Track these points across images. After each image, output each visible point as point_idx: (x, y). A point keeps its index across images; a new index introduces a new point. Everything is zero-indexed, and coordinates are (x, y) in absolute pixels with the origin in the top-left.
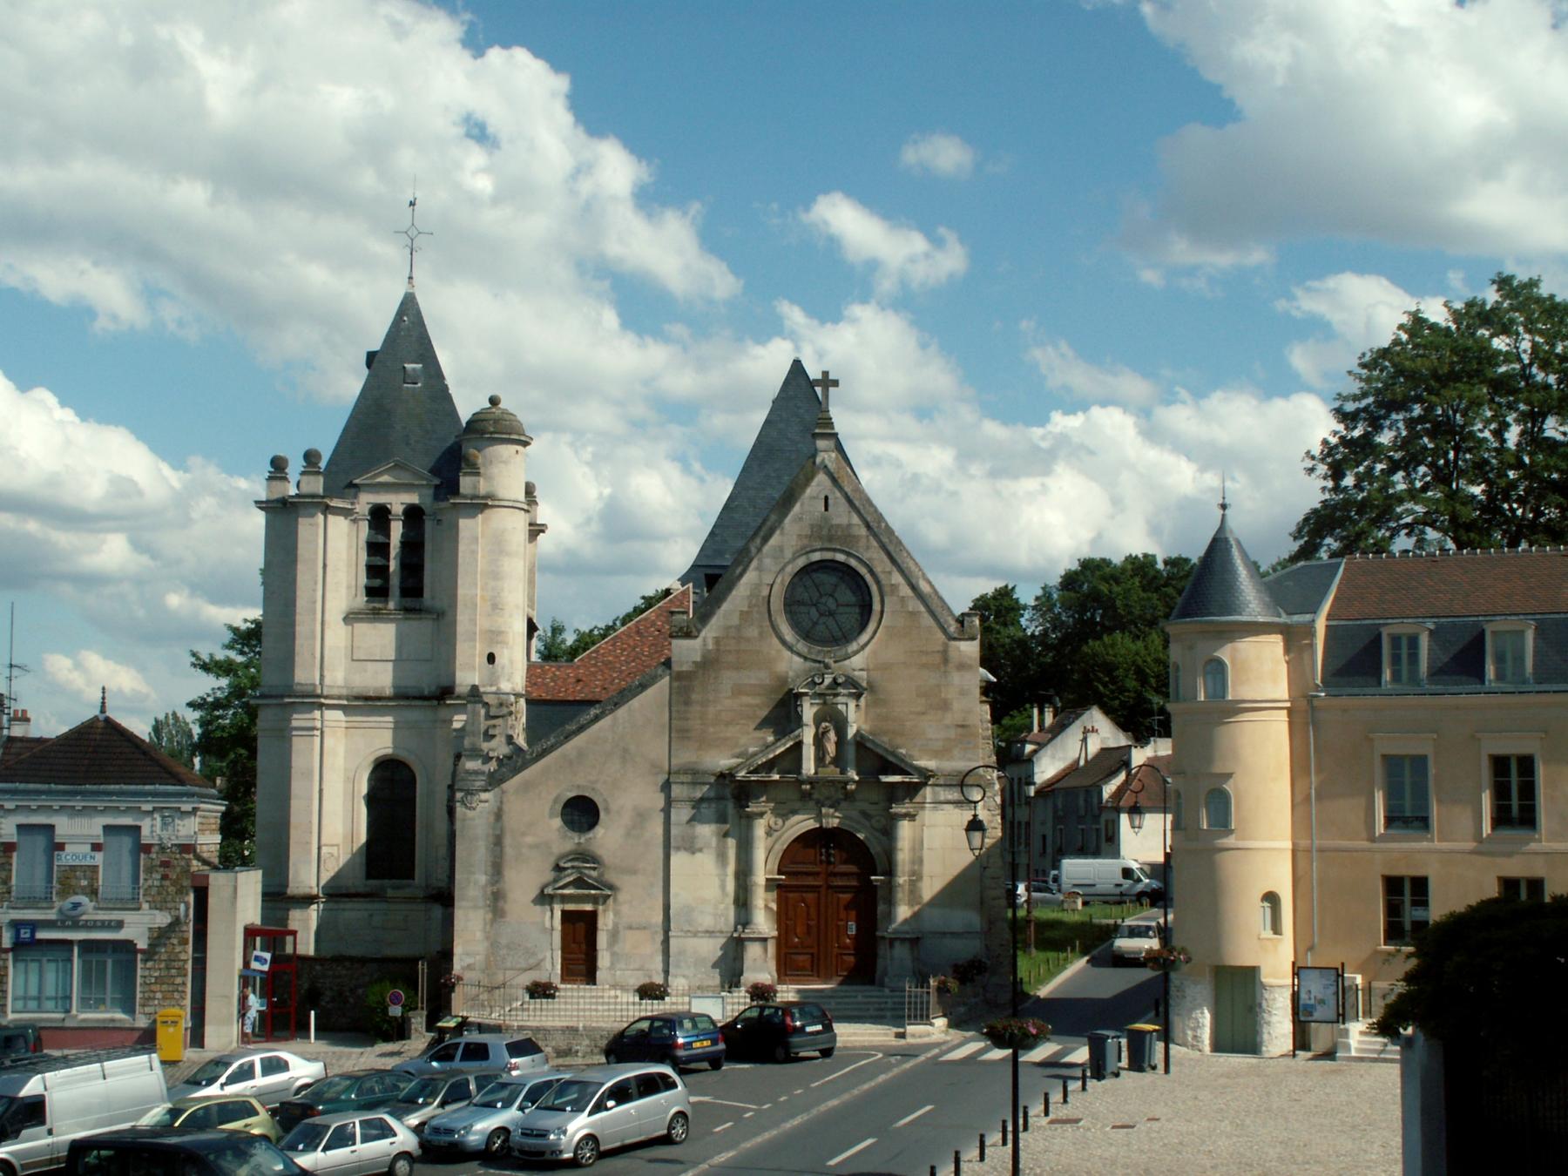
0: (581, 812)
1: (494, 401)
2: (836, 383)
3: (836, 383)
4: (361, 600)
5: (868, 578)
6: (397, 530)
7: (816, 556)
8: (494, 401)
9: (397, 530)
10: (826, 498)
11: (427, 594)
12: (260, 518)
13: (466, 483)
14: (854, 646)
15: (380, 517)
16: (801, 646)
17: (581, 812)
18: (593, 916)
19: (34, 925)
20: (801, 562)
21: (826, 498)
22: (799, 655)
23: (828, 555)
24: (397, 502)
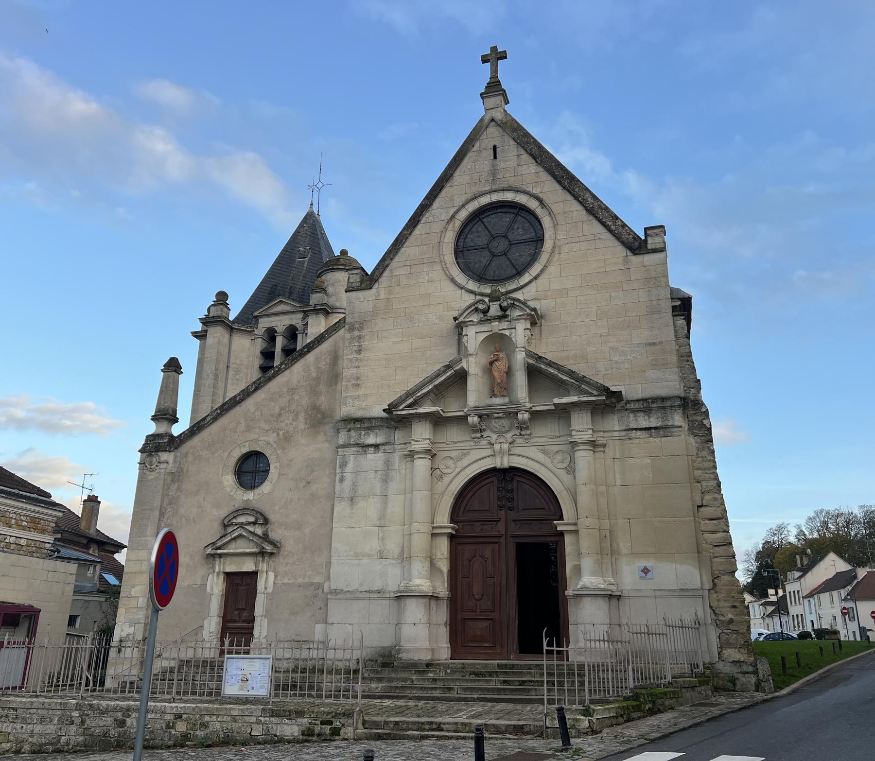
0: (251, 468)
2: (503, 56)
3: (503, 56)
5: (539, 211)
6: (280, 342)
7: (485, 200)
10: (495, 148)
14: (526, 278)
15: (271, 335)
16: (472, 285)
17: (251, 468)
18: (253, 575)
21: (495, 148)
22: (472, 292)
23: (495, 197)
24: (280, 324)
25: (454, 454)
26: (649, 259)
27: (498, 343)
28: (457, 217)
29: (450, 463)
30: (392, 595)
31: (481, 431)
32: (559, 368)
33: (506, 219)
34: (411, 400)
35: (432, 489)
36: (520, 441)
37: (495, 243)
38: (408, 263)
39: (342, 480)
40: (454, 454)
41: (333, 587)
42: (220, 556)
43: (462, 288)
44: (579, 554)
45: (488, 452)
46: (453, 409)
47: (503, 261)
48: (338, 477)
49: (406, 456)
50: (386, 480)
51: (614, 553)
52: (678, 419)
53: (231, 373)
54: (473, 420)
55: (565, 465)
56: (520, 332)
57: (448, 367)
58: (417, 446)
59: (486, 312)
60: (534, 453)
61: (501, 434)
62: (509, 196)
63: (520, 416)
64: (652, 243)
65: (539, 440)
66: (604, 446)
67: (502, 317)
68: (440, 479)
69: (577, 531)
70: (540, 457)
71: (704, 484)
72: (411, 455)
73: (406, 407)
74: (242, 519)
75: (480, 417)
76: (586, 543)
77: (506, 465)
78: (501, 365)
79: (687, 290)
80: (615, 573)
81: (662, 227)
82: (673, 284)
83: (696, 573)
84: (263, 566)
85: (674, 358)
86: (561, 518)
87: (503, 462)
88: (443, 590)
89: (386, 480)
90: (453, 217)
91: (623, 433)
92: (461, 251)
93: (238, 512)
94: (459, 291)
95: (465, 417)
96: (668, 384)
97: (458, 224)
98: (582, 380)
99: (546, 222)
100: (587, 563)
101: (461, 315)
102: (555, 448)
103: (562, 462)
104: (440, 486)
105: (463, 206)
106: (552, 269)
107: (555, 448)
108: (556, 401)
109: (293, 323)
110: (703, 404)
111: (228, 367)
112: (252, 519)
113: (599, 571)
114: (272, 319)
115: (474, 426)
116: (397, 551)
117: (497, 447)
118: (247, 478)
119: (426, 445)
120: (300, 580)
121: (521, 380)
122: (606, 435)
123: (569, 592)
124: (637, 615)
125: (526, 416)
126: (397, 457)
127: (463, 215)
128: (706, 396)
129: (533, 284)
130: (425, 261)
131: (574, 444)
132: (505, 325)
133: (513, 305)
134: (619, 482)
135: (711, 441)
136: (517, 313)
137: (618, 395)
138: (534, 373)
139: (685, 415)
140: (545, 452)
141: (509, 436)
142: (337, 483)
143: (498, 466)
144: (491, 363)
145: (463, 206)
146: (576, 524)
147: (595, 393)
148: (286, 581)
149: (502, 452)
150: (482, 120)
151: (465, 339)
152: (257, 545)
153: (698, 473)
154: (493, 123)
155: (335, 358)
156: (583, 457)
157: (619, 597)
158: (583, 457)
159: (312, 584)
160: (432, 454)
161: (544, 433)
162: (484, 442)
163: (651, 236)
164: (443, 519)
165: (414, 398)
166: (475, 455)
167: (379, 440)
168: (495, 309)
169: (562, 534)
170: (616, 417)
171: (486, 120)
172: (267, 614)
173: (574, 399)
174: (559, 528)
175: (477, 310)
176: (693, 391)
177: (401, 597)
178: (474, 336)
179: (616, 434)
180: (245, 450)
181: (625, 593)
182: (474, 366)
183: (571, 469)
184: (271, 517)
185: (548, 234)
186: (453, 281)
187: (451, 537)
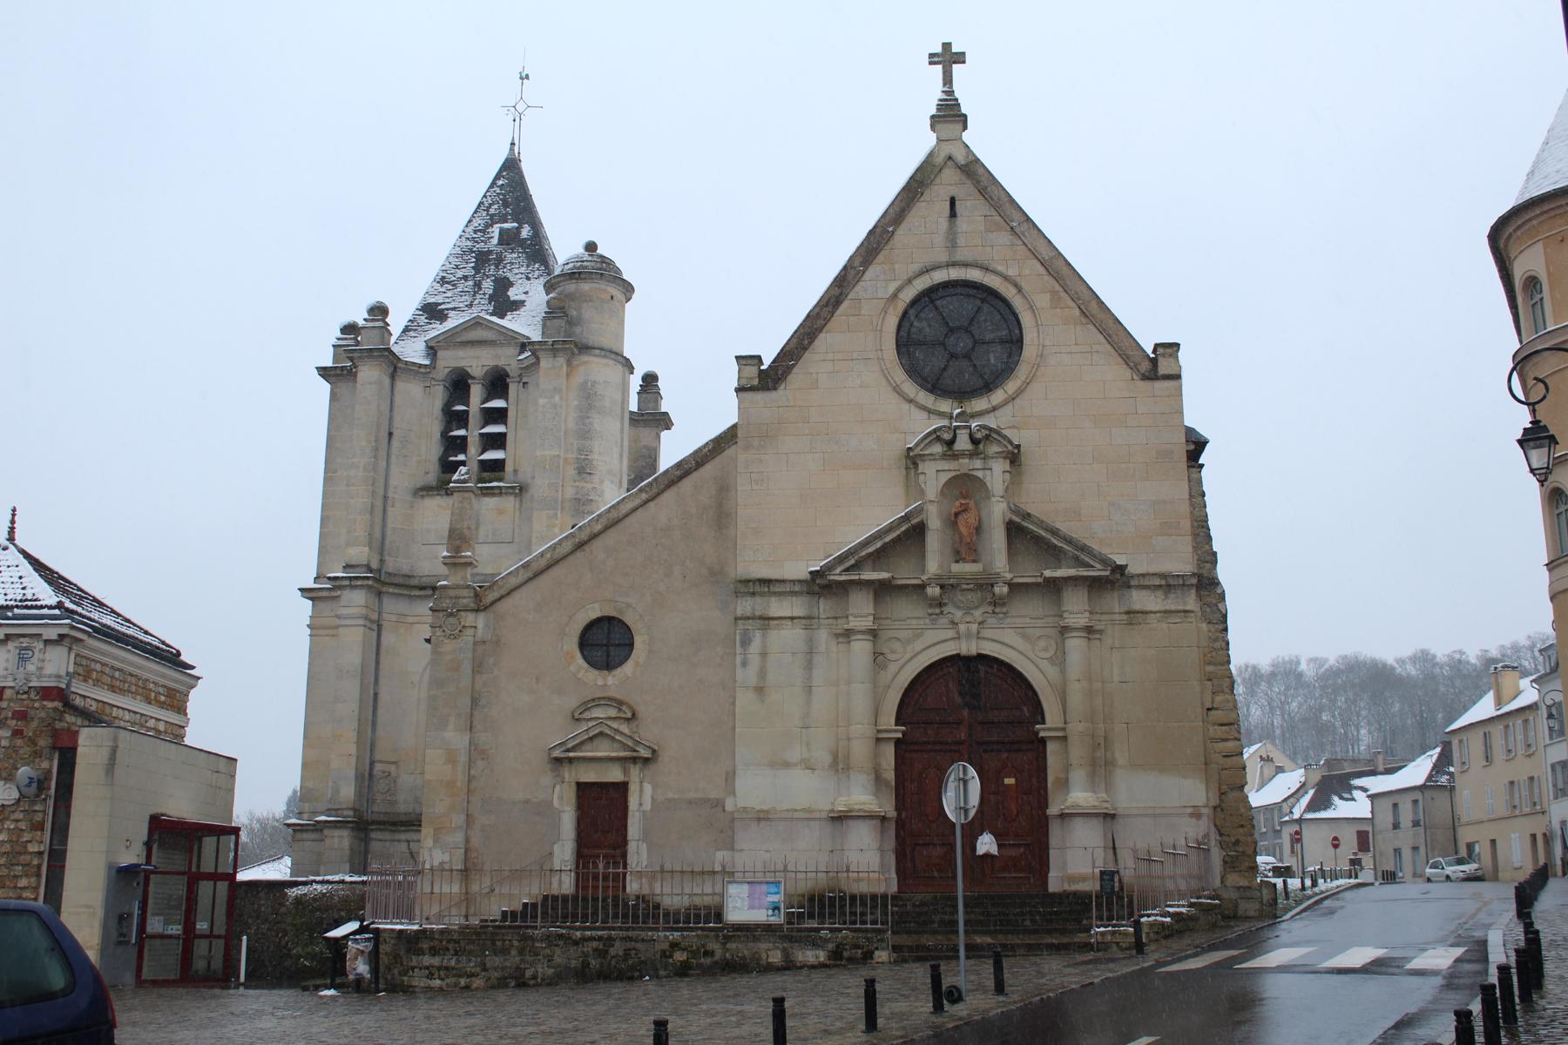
0: (606, 641)
1: (591, 247)
2: (960, 58)
3: (960, 58)
4: (432, 474)
7: (940, 276)
8: (591, 247)
10: (953, 201)
11: (509, 468)
12: (326, 387)
14: (998, 396)
17: (606, 641)
18: (622, 788)
20: (921, 284)
21: (953, 201)
23: (955, 274)
25: (903, 634)
26: (1160, 385)
27: (965, 488)
28: (901, 296)
29: (896, 645)
30: (824, 815)
31: (941, 605)
32: (1054, 532)
33: (969, 306)
34: (852, 562)
35: (874, 683)
36: (992, 621)
37: (952, 340)
38: (830, 356)
39: (744, 664)
40: (903, 634)
41: (741, 804)
42: (570, 760)
43: (910, 401)
44: (1067, 768)
45: (951, 634)
46: (905, 574)
47: (965, 363)
48: (739, 660)
49: (837, 636)
50: (809, 666)
51: (1109, 764)
52: (1191, 602)
53: (395, 443)
54: (933, 591)
55: (1048, 655)
56: (996, 475)
57: (906, 518)
58: (854, 623)
59: (950, 443)
60: (1010, 636)
61: (968, 610)
62: (974, 275)
63: (997, 590)
64: (1164, 367)
65: (1017, 620)
66: (1101, 632)
67: (973, 455)
68: (884, 667)
69: (1065, 738)
70: (1018, 642)
71: (1215, 682)
72: (848, 634)
73: (847, 570)
74: (598, 713)
75: (942, 587)
76: (1077, 751)
77: (974, 652)
78: (970, 518)
79: (1203, 431)
80: (1109, 786)
81: (1177, 345)
82: (1189, 422)
83: (1202, 787)
84: (635, 773)
85: (1186, 524)
86: (1043, 722)
87: (969, 648)
88: (888, 807)
89: (809, 666)
90: (895, 296)
91: (1125, 617)
92: (906, 344)
93: (596, 702)
94: (906, 406)
95: (922, 587)
97: (901, 306)
98: (1083, 548)
99: (1026, 320)
100: (1078, 776)
101: (917, 445)
102: (1038, 632)
103: (1046, 650)
104: (886, 676)
105: (910, 281)
106: (1036, 387)
107: (1038, 632)
108: (1048, 573)
109: (501, 363)
110: (1218, 583)
111: (390, 434)
112: (613, 713)
113: (1092, 787)
114: (461, 353)
115: (934, 599)
116: (828, 759)
117: (962, 627)
118: (599, 654)
119: (868, 623)
120: (692, 795)
121: (997, 539)
122: (1104, 617)
123: (1053, 810)
124: (1137, 837)
125: (1005, 589)
126: (823, 635)
127: (908, 295)
128: (1223, 573)
129: (1010, 406)
130: (855, 356)
131: (1064, 630)
132: (978, 463)
133: (987, 437)
134: (1116, 678)
135: (1226, 630)
136: (994, 449)
137: (1121, 569)
138: (1015, 531)
139: (1200, 597)
140: (1025, 637)
141: (978, 613)
142: (739, 670)
143: (964, 652)
144: (956, 515)
145: (910, 281)
146: (1064, 729)
147: (1098, 566)
148: (670, 795)
149: (969, 636)
150: (931, 155)
151: (921, 477)
152: (625, 747)
153: (1210, 668)
154: (950, 163)
155: (724, 489)
156: (1075, 644)
157: (1113, 816)
158: (1075, 644)
159: (706, 801)
160: (873, 634)
161: (1030, 611)
162: (943, 621)
163: (1163, 355)
164: (888, 719)
165: (856, 559)
166: (931, 636)
168: (963, 443)
169: (1043, 741)
170: (1116, 594)
171: (939, 160)
172: (646, 836)
173: (1072, 572)
174: (1042, 734)
175: (938, 439)
176: (1208, 566)
177: (840, 819)
178: (935, 476)
179: (1117, 617)
180: (594, 615)
181: (1120, 812)
182: (934, 523)
183: (1060, 659)
184: (642, 710)
185: (1029, 337)
186: (897, 390)
187: (898, 742)
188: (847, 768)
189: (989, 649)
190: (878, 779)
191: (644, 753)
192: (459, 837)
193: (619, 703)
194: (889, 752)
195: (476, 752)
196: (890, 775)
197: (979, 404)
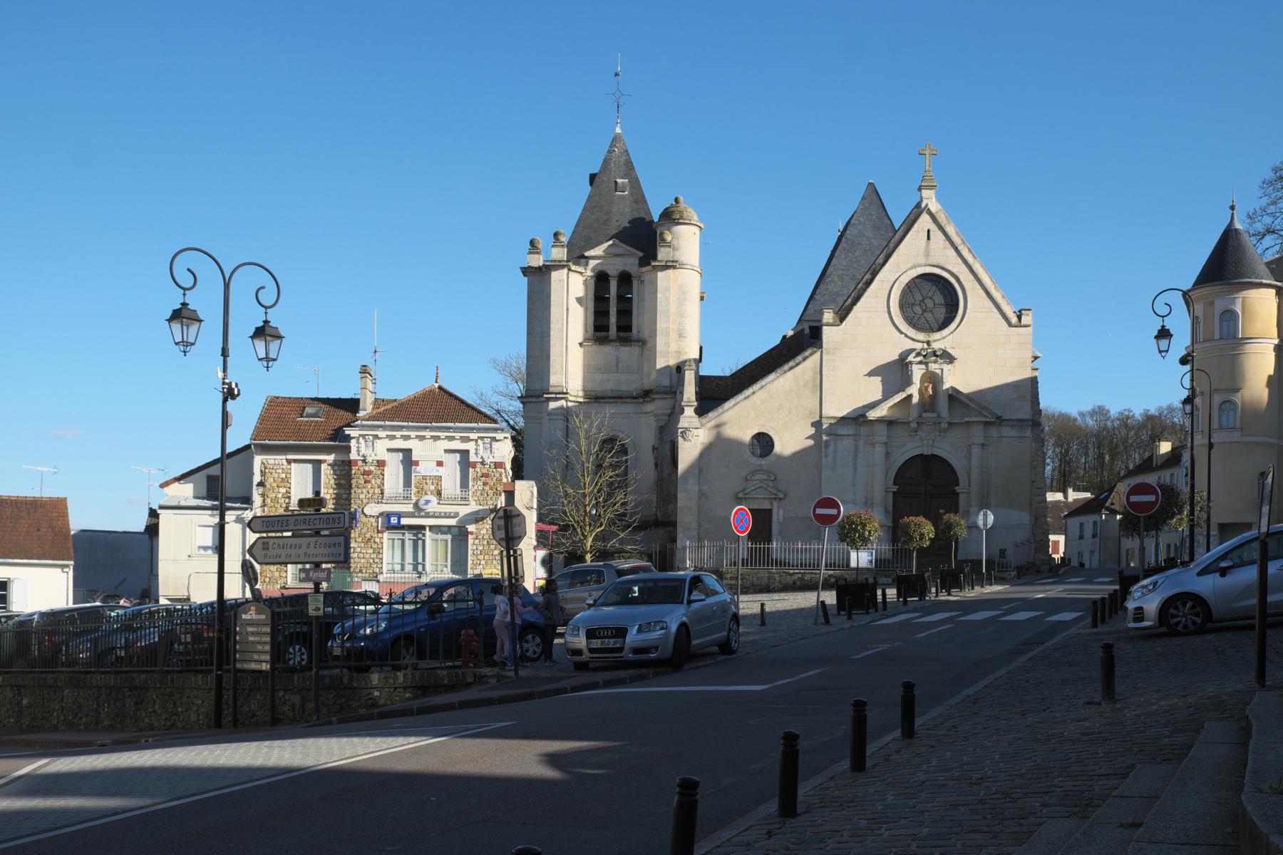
6: (613, 285)
9: (613, 285)
11: (634, 330)
13: (663, 254)
18: (770, 511)
19: (399, 515)
50: (855, 458)
52: (1028, 433)
58: (877, 438)
72: (873, 444)
74: (758, 477)
85: (1029, 396)
87: (927, 451)
89: (855, 458)
95: (908, 423)
96: (1025, 413)
109: (628, 269)
126: (861, 444)
137: (999, 418)
167: (851, 432)
188: (872, 505)
189: (937, 452)
190: (886, 511)
191: (781, 496)
192: (695, 533)
193: (768, 472)
194: (891, 496)
195: (702, 495)
196: (891, 508)
197: (937, 335)
